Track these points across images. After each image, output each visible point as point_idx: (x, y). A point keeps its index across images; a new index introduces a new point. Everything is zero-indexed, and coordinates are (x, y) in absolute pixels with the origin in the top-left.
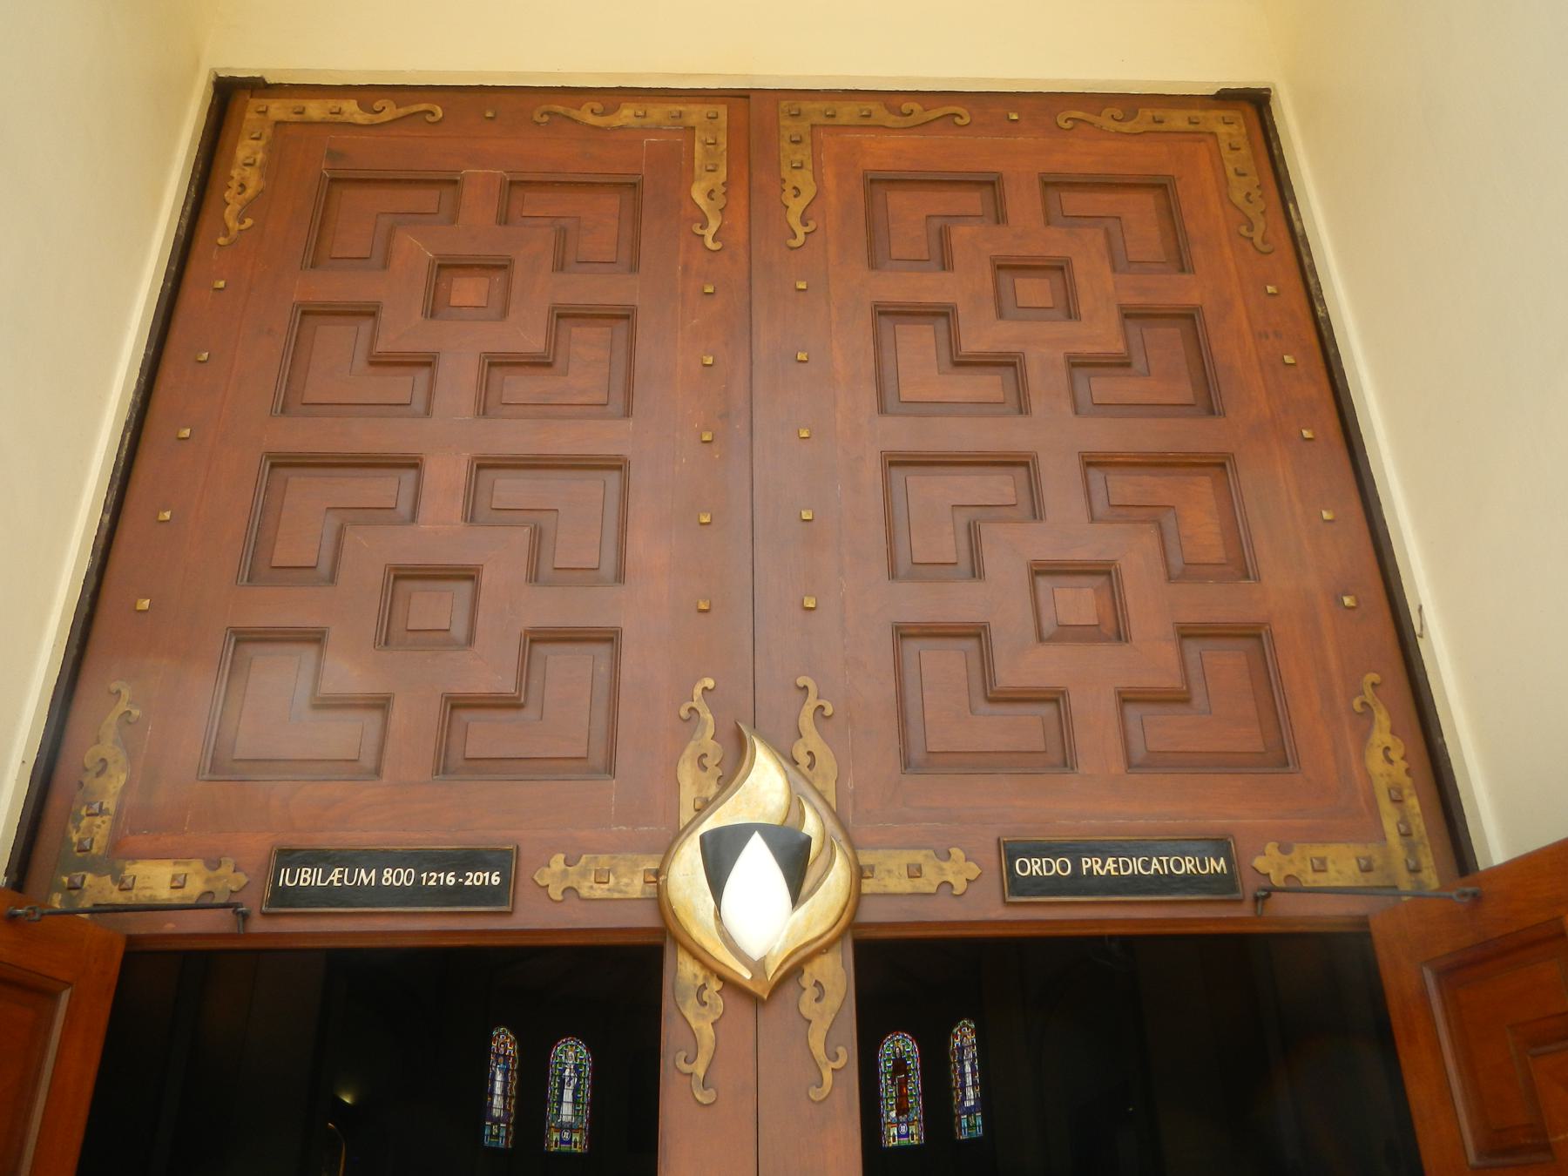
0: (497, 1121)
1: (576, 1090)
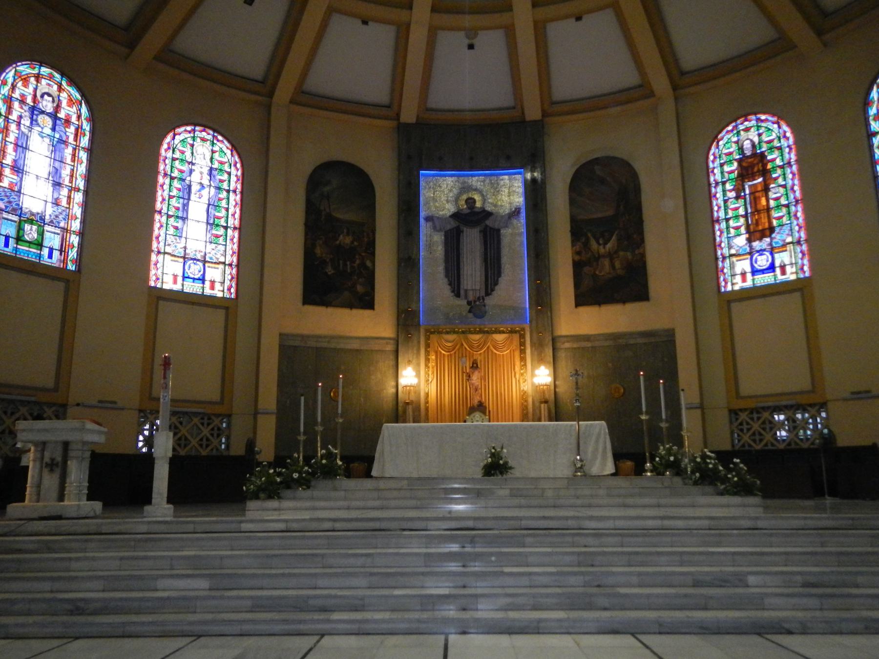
0: (39, 220)
1: (211, 205)
